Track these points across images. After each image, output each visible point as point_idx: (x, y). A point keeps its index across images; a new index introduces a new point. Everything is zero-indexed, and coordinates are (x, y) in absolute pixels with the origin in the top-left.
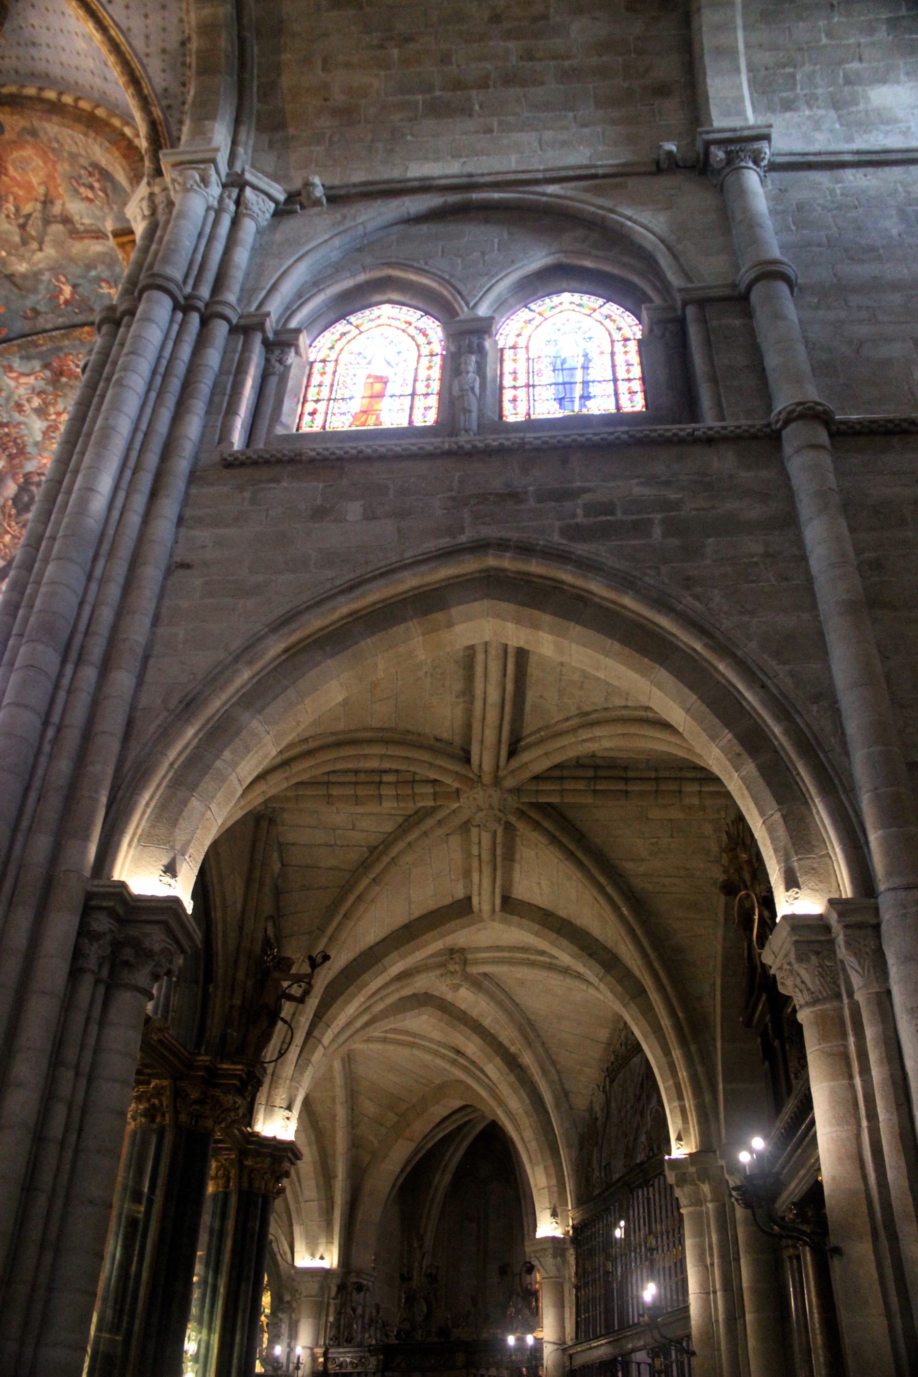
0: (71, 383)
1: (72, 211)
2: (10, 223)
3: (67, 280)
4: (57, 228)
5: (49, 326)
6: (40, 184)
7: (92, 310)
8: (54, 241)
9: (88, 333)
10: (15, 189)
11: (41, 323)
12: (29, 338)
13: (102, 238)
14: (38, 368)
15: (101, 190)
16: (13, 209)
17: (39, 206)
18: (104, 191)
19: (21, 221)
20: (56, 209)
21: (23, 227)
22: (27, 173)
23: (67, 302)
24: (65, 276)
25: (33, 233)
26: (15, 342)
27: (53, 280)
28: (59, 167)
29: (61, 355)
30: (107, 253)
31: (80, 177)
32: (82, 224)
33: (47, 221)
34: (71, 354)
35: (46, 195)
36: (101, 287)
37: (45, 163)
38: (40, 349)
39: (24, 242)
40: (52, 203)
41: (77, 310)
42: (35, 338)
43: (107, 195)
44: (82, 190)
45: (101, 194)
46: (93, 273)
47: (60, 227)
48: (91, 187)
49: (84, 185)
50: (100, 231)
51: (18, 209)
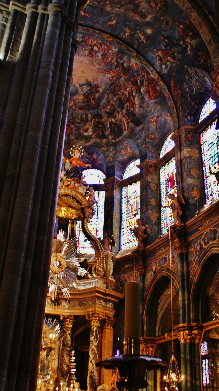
0: (84, 46)
1: (142, 5)
3: (117, 20)
4: (132, 6)
5: (97, 28)
7: (115, 31)
8: (126, 8)
9: (107, 37)
11: (96, 26)
12: (88, 28)
13: (143, 18)
14: (80, 37)
15: (159, 8)
18: (160, 8)
23: (110, 25)
24: (118, 19)
25: (123, 3)
26: (83, 27)
27: (113, 17)
29: (91, 37)
32: (141, 10)
34: (94, 38)
36: (126, 28)
38: (88, 33)
39: (117, 4)
41: (110, 29)
42: (90, 29)
44: (152, 3)
45: (158, 8)
46: (128, 23)
47: (133, 6)
48: (157, 5)
49: (155, 3)
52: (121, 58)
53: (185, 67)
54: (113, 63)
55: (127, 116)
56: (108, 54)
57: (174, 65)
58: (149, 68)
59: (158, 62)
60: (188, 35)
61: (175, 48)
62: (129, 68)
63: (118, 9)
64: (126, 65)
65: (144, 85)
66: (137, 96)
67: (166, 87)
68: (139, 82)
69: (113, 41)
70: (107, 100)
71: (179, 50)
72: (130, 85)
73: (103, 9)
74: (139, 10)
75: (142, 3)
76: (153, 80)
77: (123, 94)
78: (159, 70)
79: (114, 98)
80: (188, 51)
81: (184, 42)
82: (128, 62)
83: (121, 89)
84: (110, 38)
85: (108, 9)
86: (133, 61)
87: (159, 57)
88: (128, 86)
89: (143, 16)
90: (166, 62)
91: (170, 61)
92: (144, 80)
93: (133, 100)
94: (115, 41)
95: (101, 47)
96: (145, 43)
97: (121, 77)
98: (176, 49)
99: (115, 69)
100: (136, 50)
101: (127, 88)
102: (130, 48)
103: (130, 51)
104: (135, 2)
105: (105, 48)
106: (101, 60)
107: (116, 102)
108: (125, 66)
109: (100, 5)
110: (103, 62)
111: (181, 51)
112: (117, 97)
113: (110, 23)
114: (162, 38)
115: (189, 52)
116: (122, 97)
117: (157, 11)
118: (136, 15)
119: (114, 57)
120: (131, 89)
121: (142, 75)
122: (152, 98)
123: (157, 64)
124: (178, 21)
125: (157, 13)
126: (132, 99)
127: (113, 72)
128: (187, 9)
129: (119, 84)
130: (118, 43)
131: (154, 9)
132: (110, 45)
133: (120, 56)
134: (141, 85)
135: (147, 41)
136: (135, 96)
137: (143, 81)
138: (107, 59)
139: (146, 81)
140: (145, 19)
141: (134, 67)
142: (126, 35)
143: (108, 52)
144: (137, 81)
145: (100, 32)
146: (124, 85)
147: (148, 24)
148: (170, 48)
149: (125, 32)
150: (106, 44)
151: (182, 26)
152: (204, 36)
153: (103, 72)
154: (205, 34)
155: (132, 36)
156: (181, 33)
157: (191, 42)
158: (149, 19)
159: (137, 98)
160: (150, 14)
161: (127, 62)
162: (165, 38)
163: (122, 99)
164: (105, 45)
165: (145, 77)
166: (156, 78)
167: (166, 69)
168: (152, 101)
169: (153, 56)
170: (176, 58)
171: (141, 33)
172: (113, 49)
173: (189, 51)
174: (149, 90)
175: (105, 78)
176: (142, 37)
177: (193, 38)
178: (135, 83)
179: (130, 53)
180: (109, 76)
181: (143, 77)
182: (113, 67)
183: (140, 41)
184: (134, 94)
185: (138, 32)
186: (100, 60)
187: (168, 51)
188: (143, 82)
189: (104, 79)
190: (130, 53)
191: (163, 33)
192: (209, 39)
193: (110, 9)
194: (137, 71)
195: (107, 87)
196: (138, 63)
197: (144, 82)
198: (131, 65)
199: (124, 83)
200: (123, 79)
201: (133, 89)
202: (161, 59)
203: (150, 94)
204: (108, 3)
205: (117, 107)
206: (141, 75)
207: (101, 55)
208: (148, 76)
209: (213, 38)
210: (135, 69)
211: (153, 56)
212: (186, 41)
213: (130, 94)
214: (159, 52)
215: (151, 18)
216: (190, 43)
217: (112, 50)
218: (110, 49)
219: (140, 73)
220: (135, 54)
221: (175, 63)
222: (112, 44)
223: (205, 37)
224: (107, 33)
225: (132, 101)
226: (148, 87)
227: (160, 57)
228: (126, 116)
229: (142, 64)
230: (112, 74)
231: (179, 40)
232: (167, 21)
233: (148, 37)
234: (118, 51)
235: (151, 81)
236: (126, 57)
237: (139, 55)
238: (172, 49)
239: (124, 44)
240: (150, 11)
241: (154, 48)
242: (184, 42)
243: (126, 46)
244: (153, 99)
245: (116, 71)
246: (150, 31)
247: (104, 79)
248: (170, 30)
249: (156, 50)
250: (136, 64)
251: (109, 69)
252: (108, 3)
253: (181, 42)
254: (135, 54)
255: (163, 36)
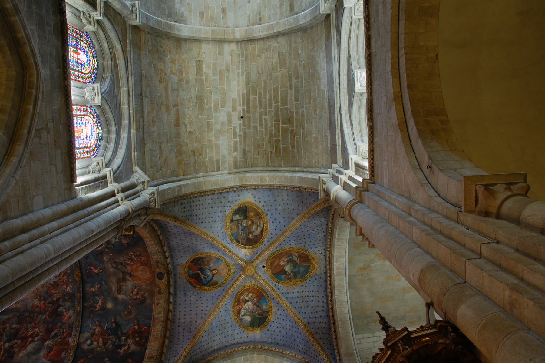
1: (127, 283)
2: (123, 260)
3: (100, 272)
6: (137, 274)
9: (78, 274)
10: (135, 266)
15: (137, 298)
16: (128, 263)
17: (129, 272)
18: (136, 299)
19: (124, 264)
20: (128, 278)
21: (121, 264)
22: (142, 272)
24: (101, 272)
25: (119, 266)
28: (144, 284)
30: (112, 292)
31: (141, 291)
33: (123, 272)
35: (133, 275)
36: (97, 284)
37: (145, 279)
39: (115, 262)
40: (130, 277)
43: (135, 299)
44: (136, 290)
45: (135, 297)
46: (103, 283)
47: (121, 276)
48: (137, 294)
49: (138, 292)
50: (121, 292)
51: (128, 264)
52: (64, 300)
53: (107, 359)
54: (54, 298)
55: (4, 351)
56: (60, 287)
57: (99, 349)
58: (76, 331)
59: (89, 333)
60: (134, 337)
61: (115, 337)
62: (61, 314)
63: (111, 266)
64: (61, 310)
65: (55, 340)
66: (36, 343)
67: (72, 360)
68: (53, 333)
69: (77, 282)
70: (6, 319)
71: (115, 341)
72: (43, 328)
73: (102, 255)
74: (122, 283)
75: (130, 282)
76: (68, 343)
77: (27, 329)
78: (82, 340)
79: (15, 324)
80: (121, 350)
81: (126, 340)
82: (66, 310)
83: (31, 323)
84: (78, 278)
85: (106, 259)
86: (71, 312)
87: (94, 331)
88: (41, 327)
89: (119, 291)
90: (95, 341)
91: (98, 343)
92: (60, 337)
93: (28, 343)
94: (78, 284)
95: (63, 276)
96: (96, 309)
97: (45, 314)
98: (114, 339)
99: (49, 303)
100: (83, 307)
101: (36, 328)
102: (81, 301)
103: (79, 303)
104: (127, 276)
105: (64, 280)
106: (49, 284)
107: (10, 329)
108: (59, 310)
109: (105, 250)
110: (48, 288)
111: (116, 343)
112: (19, 326)
113: (93, 268)
114: (113, 320)
115: (122, 351)
116: (22, 331)
117: (132, 298)
118: (116, 285)
119: (61, 294)
120: (39, 332)
121: (63, 330)
122: (48, 358)
123: (87, 335)
124: (138, 321)
125: (131, 299)
126: (29, 341)
127: (44, 303)
128: (157, 319)
129: (35, 318)
130: (79, 287)
131: (132, 295)
132: (71, 282)
133: (66, 298)
134: (52, 338)
135: (99, 310)
136: (35, 341)
137: (58, 336)
138: (54, 289)
139: (60, 339)
140: (119, 294)
141: (64, 318)
142: (91, 289)
143: (62, 285)
144: (53, 331)
145: (78, 265)
146: (38, 323)
147: (115, 299)
148: (110, 333)
149: (94, 287)
150: (70, 279)
151: (136, 327)
152: (151, 349)
153: (36, 294)
154: (153, 348)
155: (94, 294)
156: (131, 332)
157: (131, 344)
158: (121, 297)
159: (34, 345)
160: (125, 295)
161: (65, 308)
162: (115, 322)
163: (20, 333)
164: (67, 278)
165: (63, 333)
166: (72, 344)
167: (89, 345)
168: (46, 360)
169: (91, 325)
170: (106, 346)
171: (102, 300)
172: (69, 288)
173: (123, 350)
174: (53, 348)
175: (30, 301)
176: (100, 304)
177: (136, 343)
178: (49, 331)
179: (77, 304)
180: (36, 302)
181: (62, 333)
182: (50, 300)
183: (95, 305)
184: (36, 339)
185: (102, 297)
186: (48, 283)
187: (106, 334)
188: (57, 337)
189: (29, 301)
190: (77, 304)
191: (118, 317)
192: (153, 355)
193: (106, 260)
194: (65, 323)
195: (22, 309)
196: (72, 318)
197: (58, 338)
198: (65, 313)
199: (40, 321)
200: (44, 316)
201: (40, 334)
202: (93, 334)
203: (50, 352)
204: (111, 255)
205: (5, 335)
206: (62, 330)
207: (54, 282)
208: (66, 337)
209: (157, 357)
210: (64, 320)
211: (91, 325)
212: (129, 340)
213: (32, 336)
214: (98, 327)
215: (123, 299)
216: (129, 345)
217: (67, 288)
218: (67, 285)
219: (63, 327)
220: (79, 309)
221: (101, 349)
222: (73, 283)
223: (151, 350)
224: (81, 273)
225: (26, 343)
226: (56, 345)
227: (95, 332)
228: (3, 351)
229: (74, 322)
230: (40, 304)
231: (123, 334)
232: (131, 312)
233: (103, 308)
234: (70, 293)
235: (64, 344)
236: (69, 304)
237: (81, 313)
238: (111, 335)
239: (81, 292)
240: (128, 293)
241: (98, 321)
242: (126, 340)
243: (80, 296)
244: (48, 359)
245: (47, 305)
246: (111, 306)
247: (29, 301)
248: (125, 320)
249: (98, 323)
250: (70, 317)
251: (44, 297)
252: (111, 255)
253: (123, 338)
254: (79, 309)
255: (115, 320)
